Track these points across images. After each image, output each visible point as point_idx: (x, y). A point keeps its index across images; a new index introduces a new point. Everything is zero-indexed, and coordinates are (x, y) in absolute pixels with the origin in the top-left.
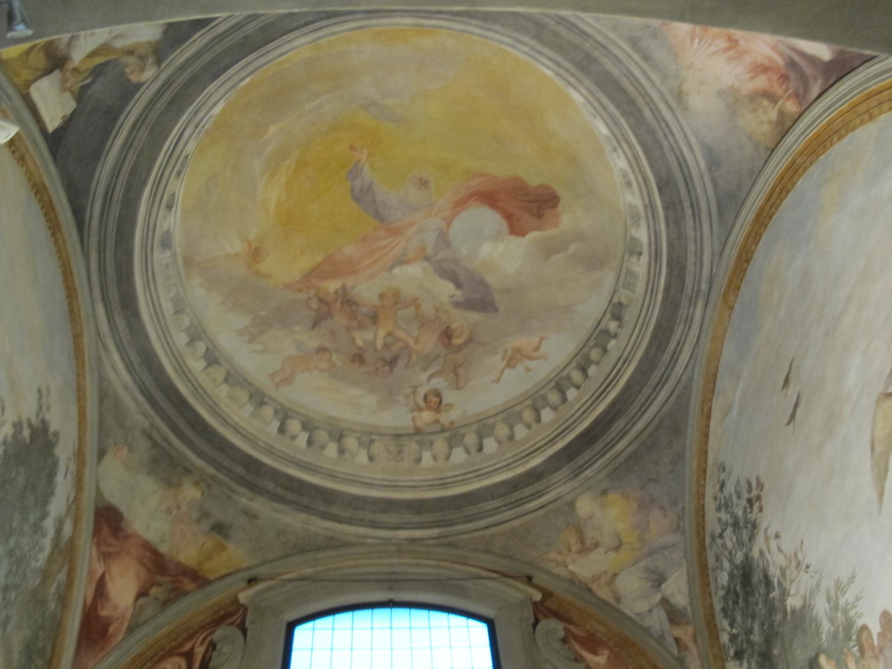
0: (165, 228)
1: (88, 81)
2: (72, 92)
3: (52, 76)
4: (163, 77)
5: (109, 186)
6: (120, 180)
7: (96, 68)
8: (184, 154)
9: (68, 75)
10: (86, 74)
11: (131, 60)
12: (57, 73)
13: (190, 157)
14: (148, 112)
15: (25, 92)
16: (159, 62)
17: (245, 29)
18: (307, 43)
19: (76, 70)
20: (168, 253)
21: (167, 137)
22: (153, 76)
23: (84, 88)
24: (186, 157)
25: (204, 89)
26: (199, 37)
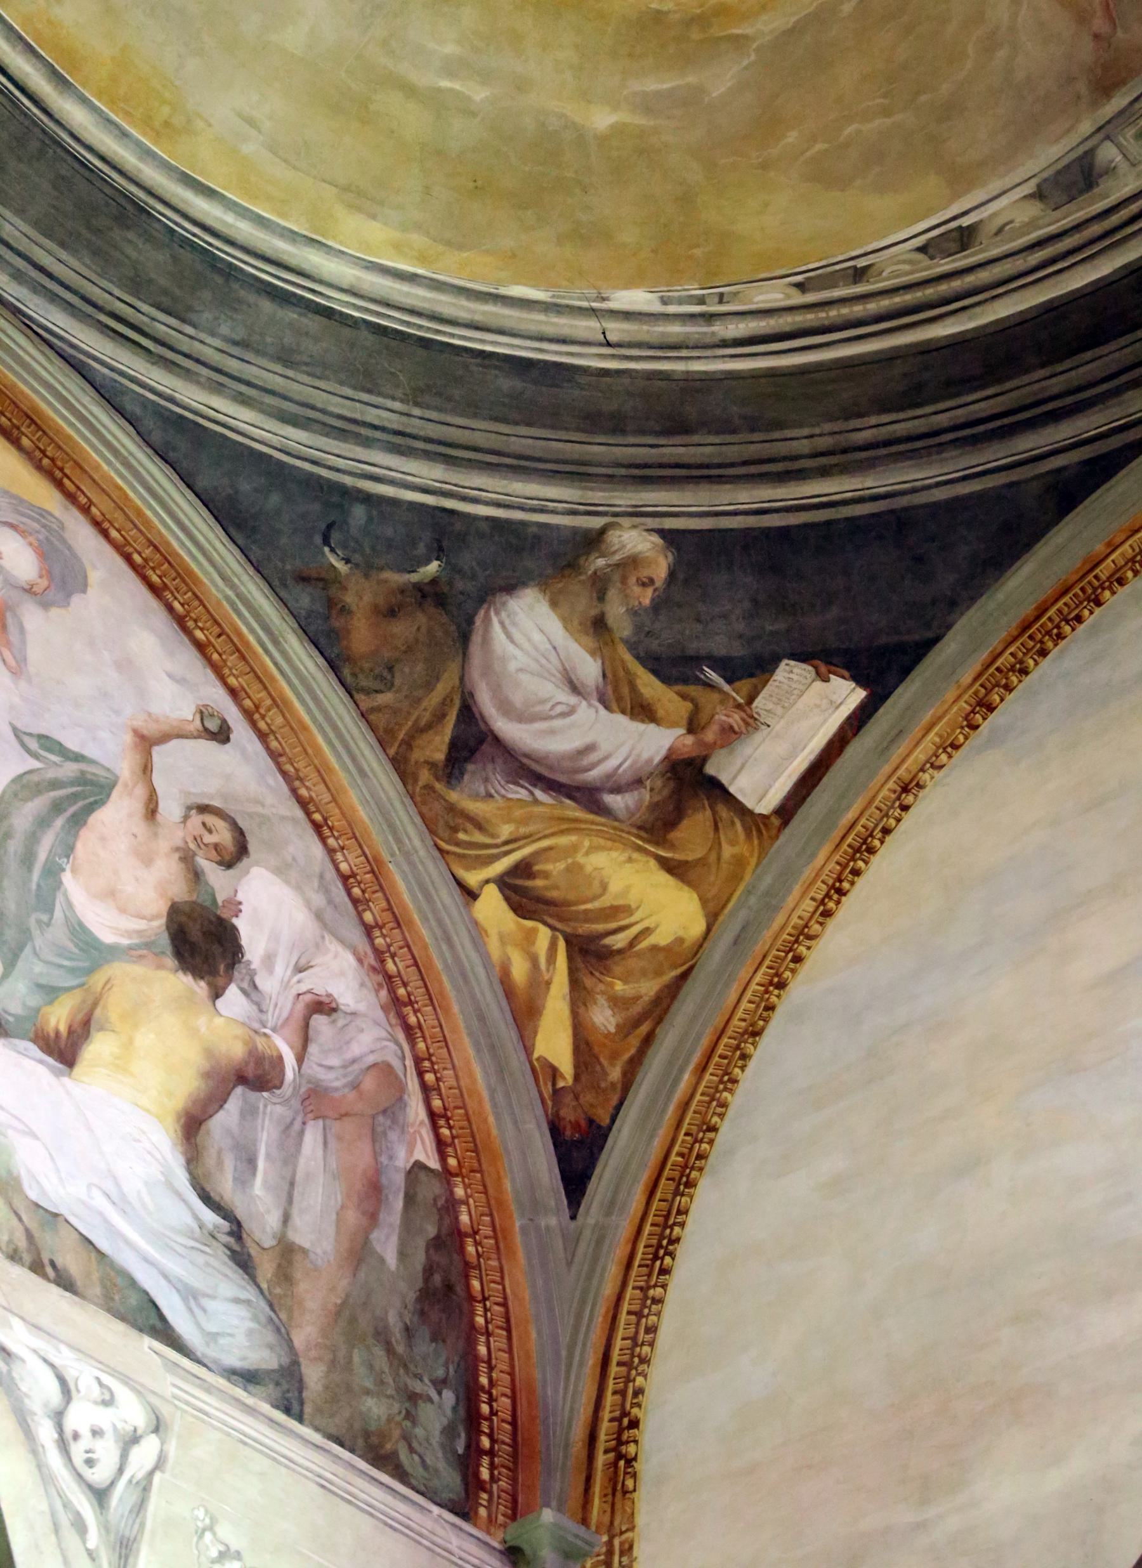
0: (1034, 209)
1: (713, 676)
2: (751, 700)
3: (724, 779)
4: (625, 498)
5: (974, 441)
6: (943, 420)
7: (667, 680)
8: (799, 299)
9: (710, 735)
10: (693, 690)
11: (616, 611)
12: (710, 769)
13: (799, 278)
14: (732, 465)
15: (776, 822)
16: (593, 541)
17: (393, 421)
18: (328, 249)
19: (693, 726)
20: (1108, 153)
21: (772, 374)
22: (634, 527)
23: (732, 670)
24: (801, 287)
25: (606, 372)
26: (475, 501)
